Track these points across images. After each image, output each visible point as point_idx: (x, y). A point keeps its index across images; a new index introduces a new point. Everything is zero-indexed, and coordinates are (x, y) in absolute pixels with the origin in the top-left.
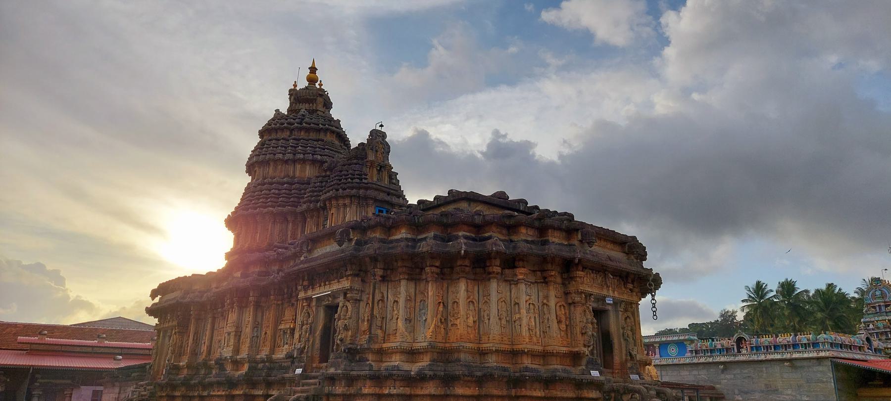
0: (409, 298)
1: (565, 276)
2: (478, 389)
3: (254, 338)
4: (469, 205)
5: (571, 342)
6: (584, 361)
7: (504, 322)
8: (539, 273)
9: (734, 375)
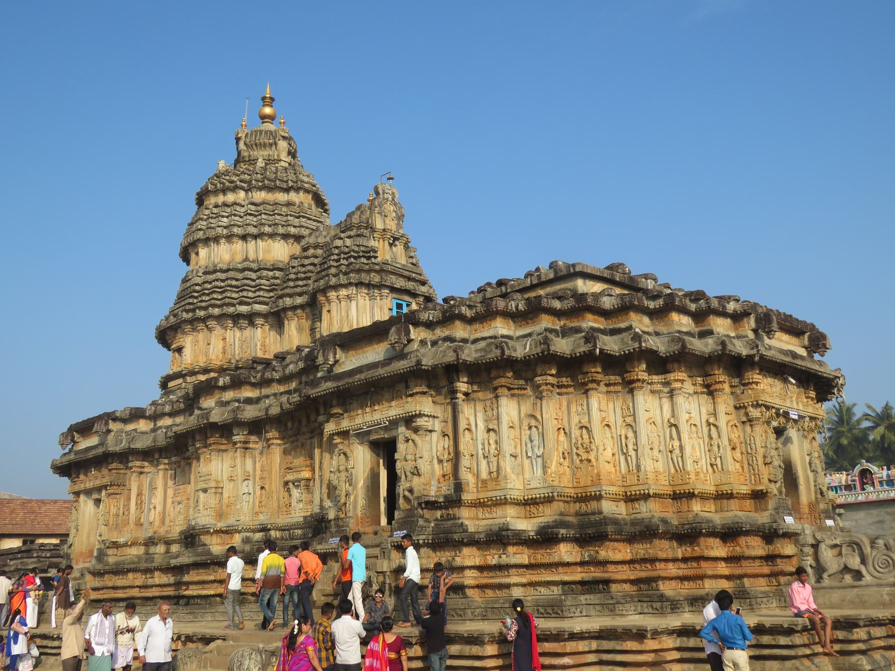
0: (511, 425)
1: (736, 381)
4: (584, 283)
5: (750, 477)
6: (771, 504)
7: (656, 452)
8: (699, 380)
9: (856, 521)
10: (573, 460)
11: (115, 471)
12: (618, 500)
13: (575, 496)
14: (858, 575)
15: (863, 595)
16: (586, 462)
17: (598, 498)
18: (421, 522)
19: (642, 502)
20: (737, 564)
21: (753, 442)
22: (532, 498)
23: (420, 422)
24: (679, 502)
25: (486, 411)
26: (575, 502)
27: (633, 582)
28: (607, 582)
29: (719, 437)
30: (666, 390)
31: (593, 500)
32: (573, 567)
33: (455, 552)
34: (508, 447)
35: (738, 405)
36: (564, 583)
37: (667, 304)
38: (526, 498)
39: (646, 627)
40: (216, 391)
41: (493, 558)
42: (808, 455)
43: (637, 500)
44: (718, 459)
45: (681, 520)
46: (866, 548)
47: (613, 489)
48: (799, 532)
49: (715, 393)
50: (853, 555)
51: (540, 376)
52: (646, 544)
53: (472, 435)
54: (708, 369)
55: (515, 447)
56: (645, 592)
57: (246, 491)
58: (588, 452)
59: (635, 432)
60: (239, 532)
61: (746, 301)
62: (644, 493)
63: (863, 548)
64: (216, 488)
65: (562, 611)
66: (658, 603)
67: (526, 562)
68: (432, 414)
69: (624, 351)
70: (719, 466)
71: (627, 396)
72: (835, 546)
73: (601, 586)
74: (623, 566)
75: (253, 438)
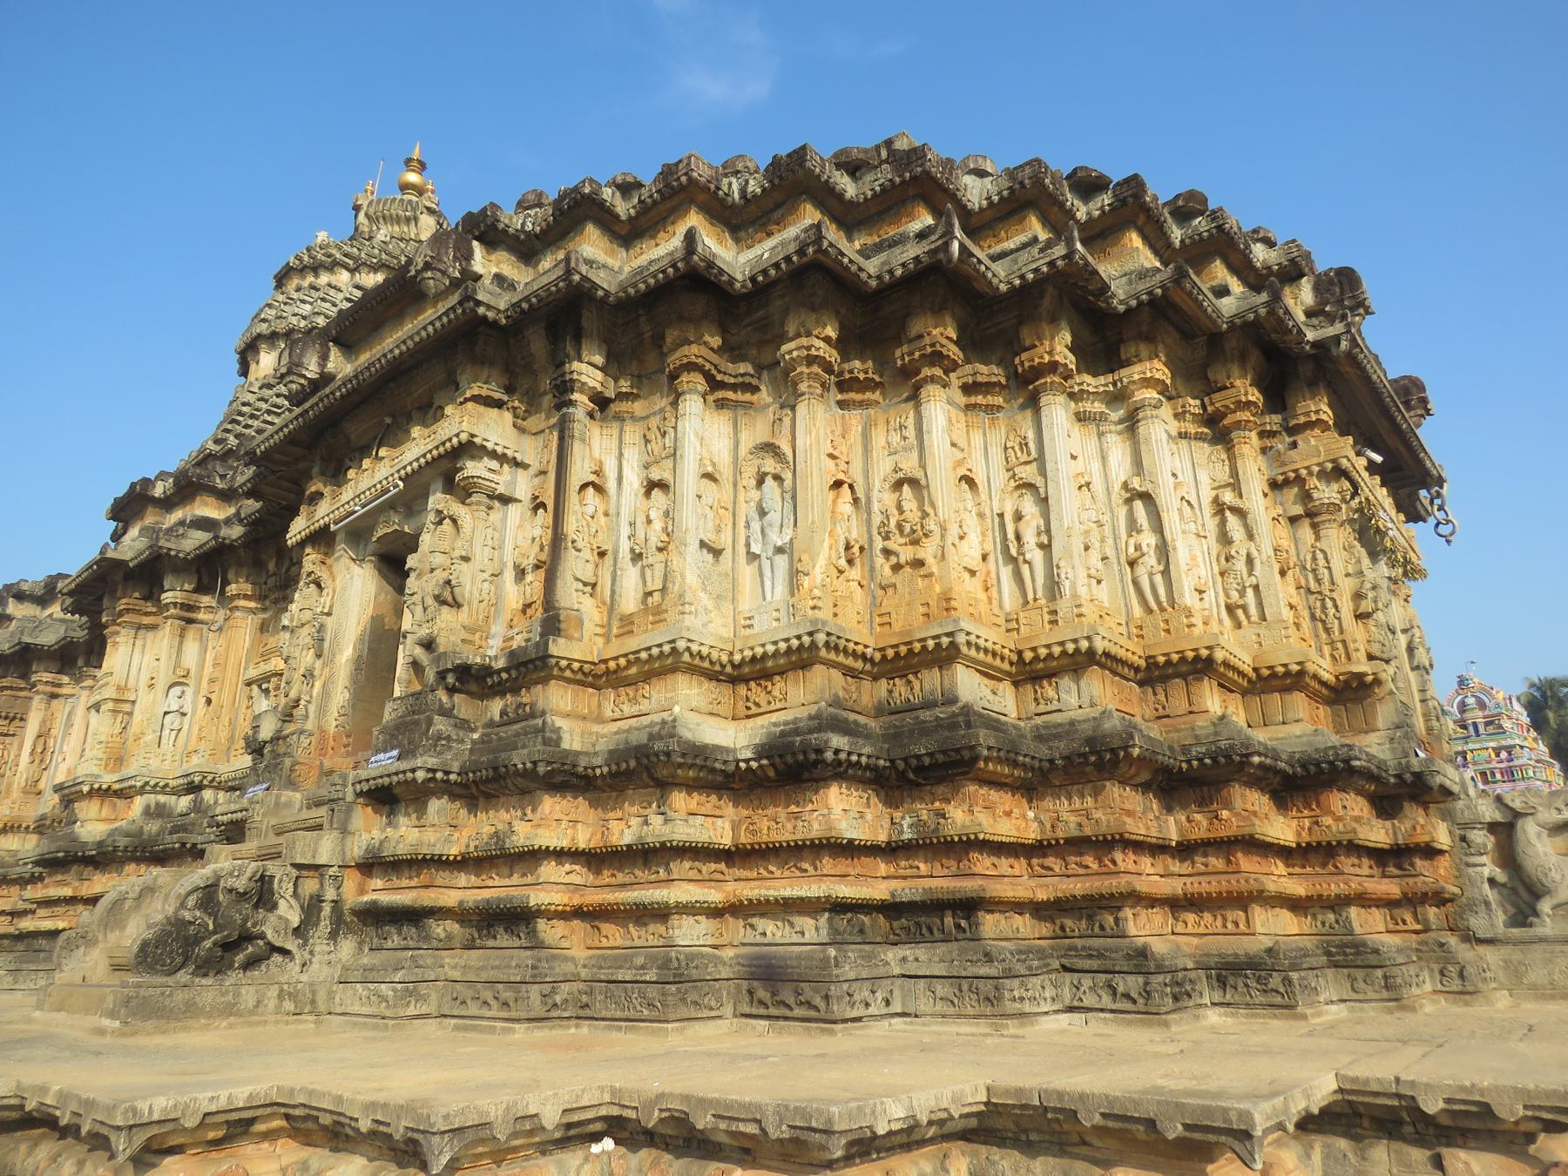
0: (710, 469)
1: (1274, 421)
2: (1036, 818)
3: (168, 717)
8: (1193, 404)
10: (872, 569)
11: (9, 692)
13: (878, 656)
16: (908, 569)
17: (944, 655)
18: (440, 725)
19: (1066, 682)
20: (1324, 865)
21: (1321, 562)
22: (754, 659)
23: (473, 468)
24: (1160, 690)
25: (647, 441)
26: (875, 678)
27: (1039, 910)
28: (969, 907)
29: (1251, 537)
30: (1116, 415)
31: (929, 665)
32: (865, 860)
33: (523, 809)
34: (695, 520)
35: (1281, 478)
36: (839, 907)
37: (1123, 202)
38: (737, 658)
39: (1246, 1116)
40: (150, 509)
41: (625, 828)
42: (1405, 631)
43: (1051, 675)
44: (1250, 592)
45: (1175, 735)
47: (991, 636)
49: (1233, 435)
51: (792, 339)
52: (1082, 796)
53: (608, 503)
54: (1217, 374)
55: (718, 530)
56: (1079, 943)
57: (174, 707)
58: (915, 542)
59: (1044, 502)
60: (142, 791)
61: (1294, 241)
62: (1077, 650)
64: (116, 701)
65: (827, 998)
66: (1131, 979)
67: (725, 840)
68: (510, 453)
69: (1022, 277)
70: (1253, 610)
71: (1019, 417)
73: (949, 920)
74: (1011, 860)
75: (206, 600)
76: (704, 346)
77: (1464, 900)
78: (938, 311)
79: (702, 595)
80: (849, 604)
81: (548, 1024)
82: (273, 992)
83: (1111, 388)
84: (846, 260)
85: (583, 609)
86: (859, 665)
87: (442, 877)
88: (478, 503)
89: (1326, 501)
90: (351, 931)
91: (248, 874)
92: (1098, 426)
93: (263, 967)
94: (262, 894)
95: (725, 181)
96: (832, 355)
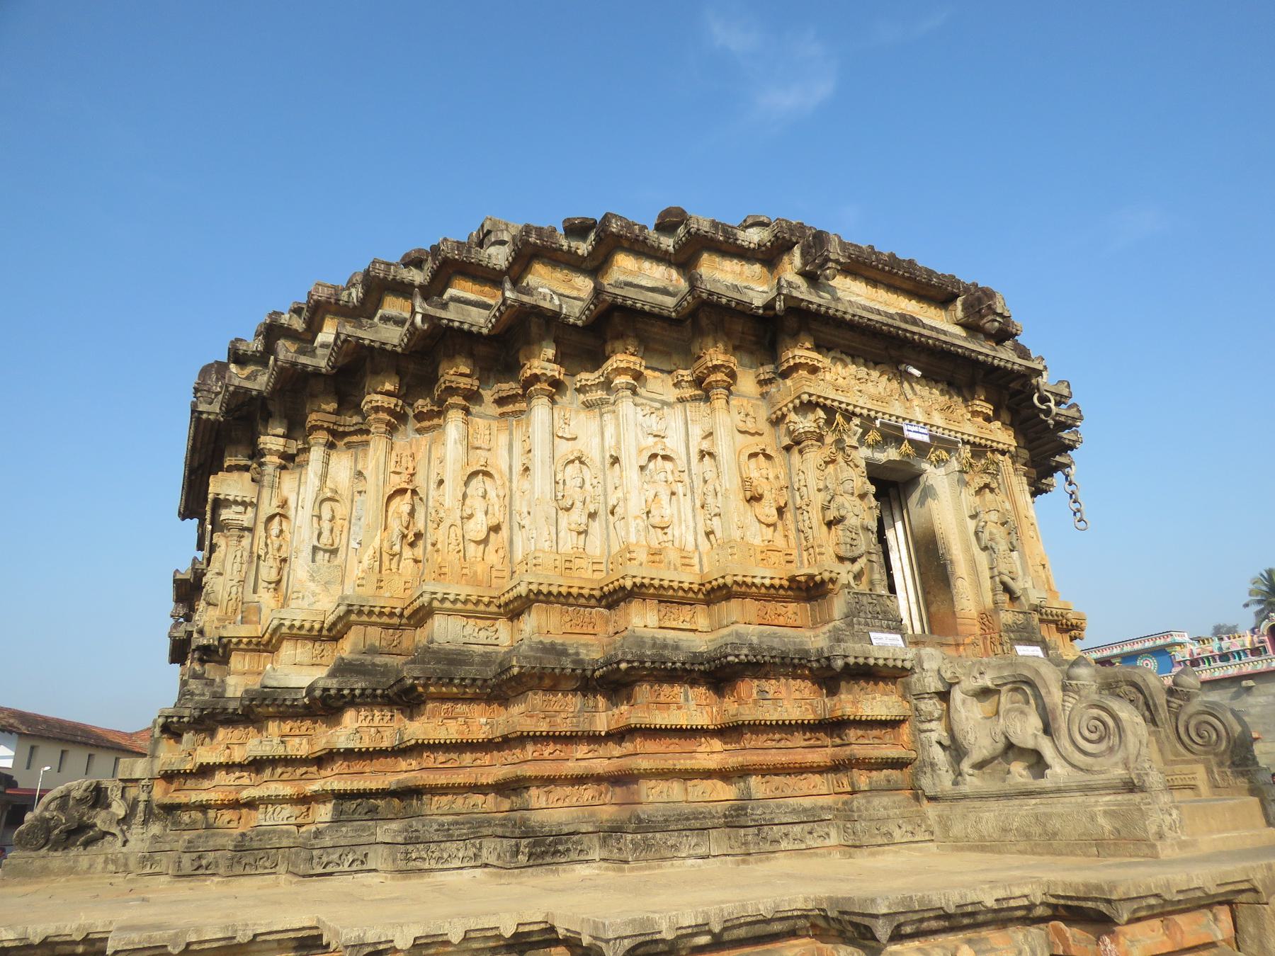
0: (329, 495)
1: (767, 371)
5: (801, 556)
6: (839, 605)
8: (686, 374)
12: (494, 617)
14: (1037, 763)
15: (1049, 816)
23: (226, 514)
35: (774, 416)
42: (973, 517)
46: (1049, 692)
48: (908, 665)
50: (1022, 712)
63: (1043, 692)
72: (984, 693)
76: (322, 412)
77: (917, 762)
78: (451, 357)
79: (311, 584)
80: (396, 577)
81: (194, 878)
82: (101, 859)
83: (602, 379)
84: (367, 342)
85: (261, 600)
86: (396, 621)
87: (190, 783)
88: (232, 536)
89: (802, 431)
90: (158, 818)
91: (84, 787)
92: (600, 409)
93: (100, 844)
94: (98, 798)
95: (345, 293)
96: (391, 402)
